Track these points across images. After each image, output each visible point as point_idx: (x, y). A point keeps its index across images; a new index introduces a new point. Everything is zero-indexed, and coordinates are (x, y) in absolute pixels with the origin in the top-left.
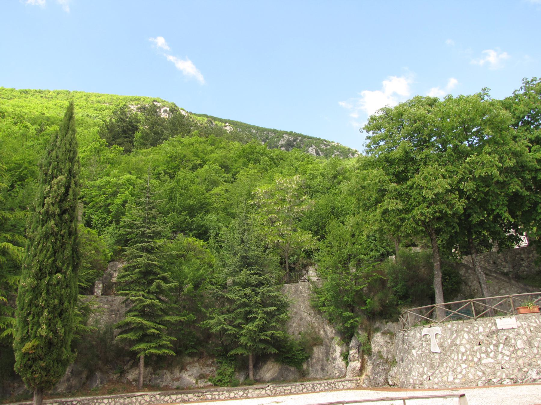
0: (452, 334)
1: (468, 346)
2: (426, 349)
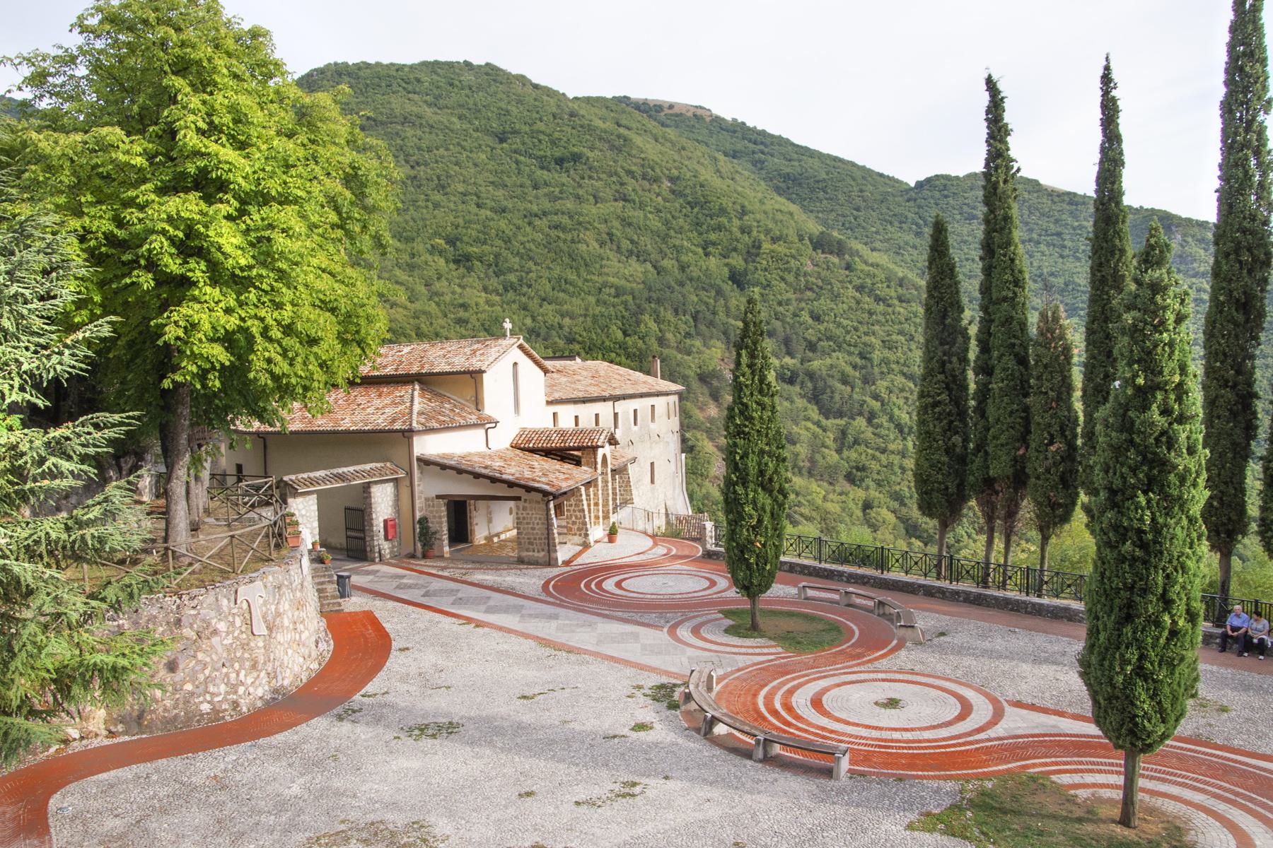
0: (274, 597)
1: (290, 614)
2: (242, 632)
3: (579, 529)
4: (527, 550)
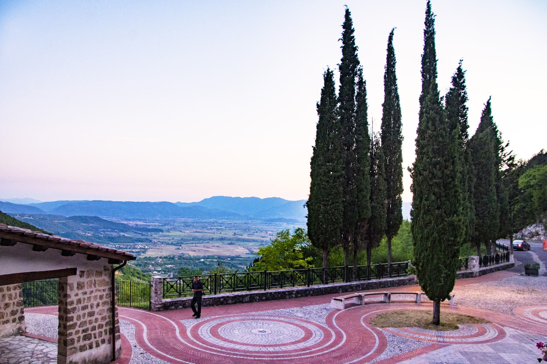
3: (13, 313)
4: (82, 349)
